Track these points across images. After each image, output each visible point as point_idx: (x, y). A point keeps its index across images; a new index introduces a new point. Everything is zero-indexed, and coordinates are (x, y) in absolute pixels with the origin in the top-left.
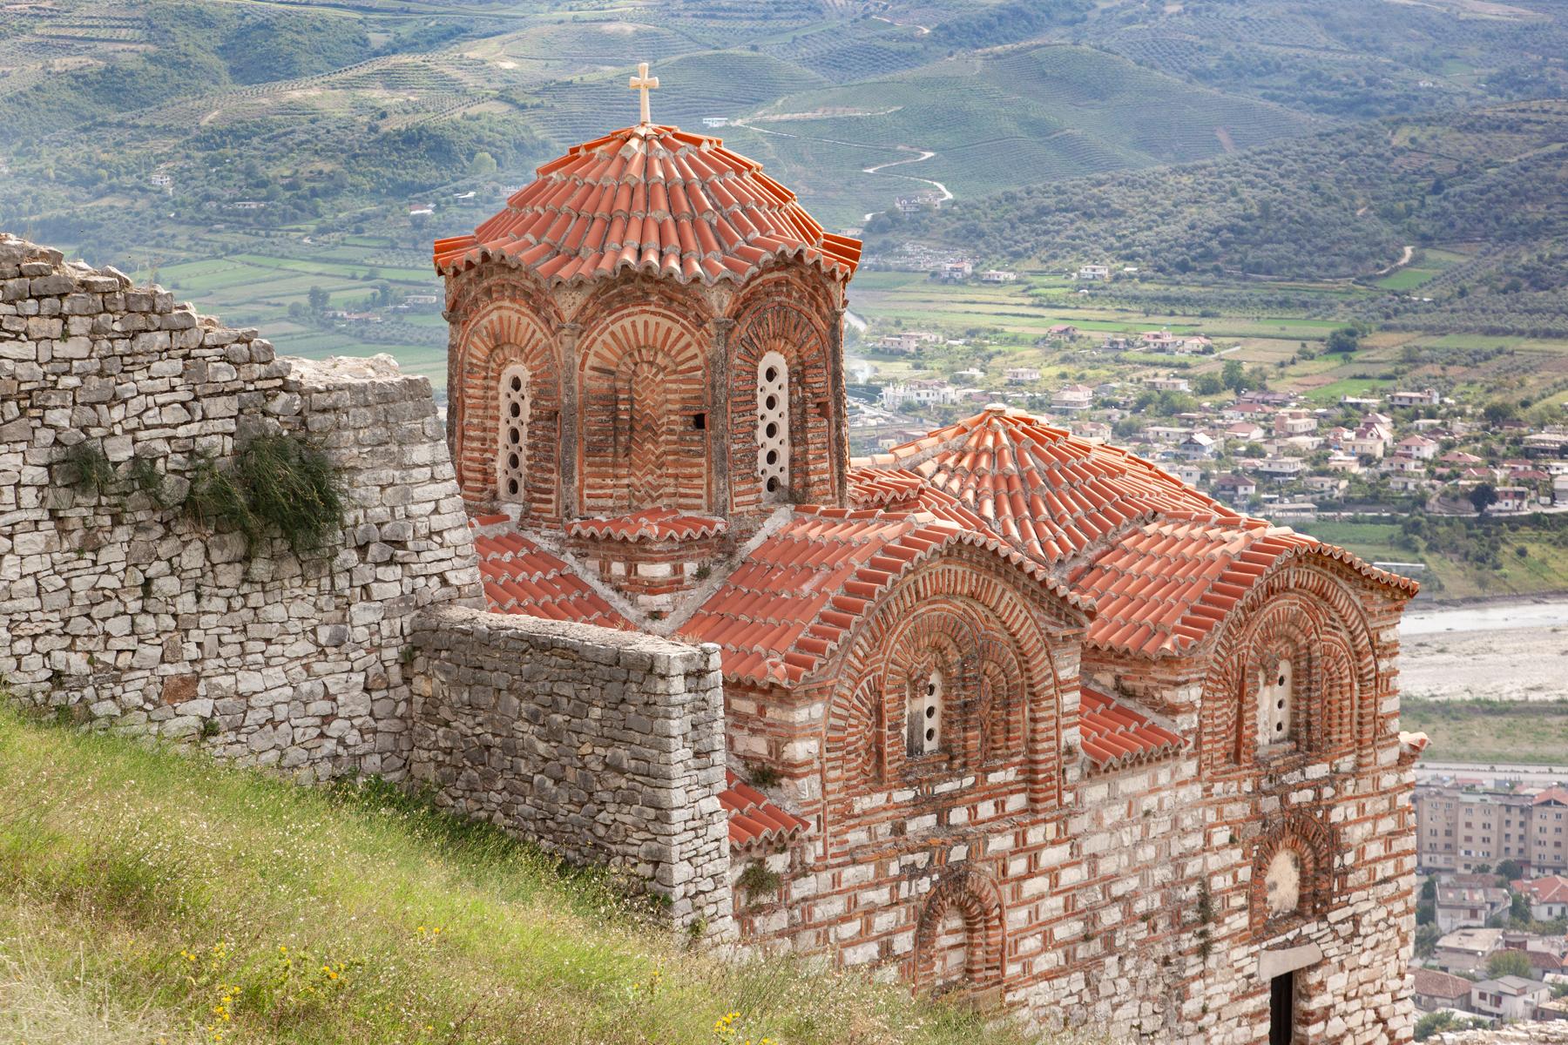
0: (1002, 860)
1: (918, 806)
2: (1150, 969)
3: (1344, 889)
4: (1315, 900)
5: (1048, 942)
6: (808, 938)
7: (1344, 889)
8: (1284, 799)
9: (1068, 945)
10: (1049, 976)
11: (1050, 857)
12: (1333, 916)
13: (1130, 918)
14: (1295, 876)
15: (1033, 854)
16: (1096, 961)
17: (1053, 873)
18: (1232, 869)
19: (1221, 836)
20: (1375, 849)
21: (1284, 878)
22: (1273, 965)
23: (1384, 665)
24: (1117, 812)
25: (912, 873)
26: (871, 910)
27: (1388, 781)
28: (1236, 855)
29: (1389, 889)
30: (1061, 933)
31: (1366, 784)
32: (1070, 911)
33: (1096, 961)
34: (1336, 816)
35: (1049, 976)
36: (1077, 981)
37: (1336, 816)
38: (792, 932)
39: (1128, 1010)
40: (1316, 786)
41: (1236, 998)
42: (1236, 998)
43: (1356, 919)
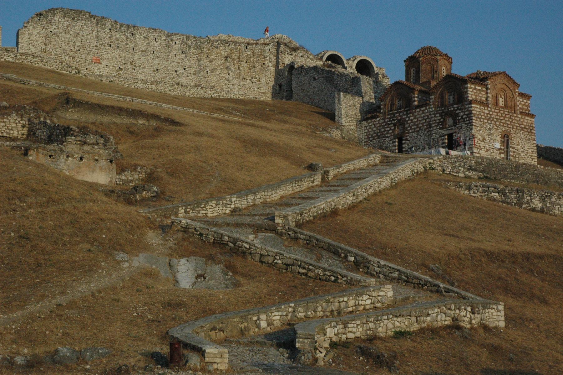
0: (405, 119)
1: (397, 113)
2: (426, 132)
3: (459, 122)
4: (455, 124)
5: (411, 129)
6: (381, 127)
7: (459, 122)
8: (448, 109)
9: (414, 129)
10: (412, 132)
11: (412, 118)
12: (457, 126)
13: (423, 126)
14: (452, 121)
15: (409, 117)
16: (418, 131)
17: (411, 120)
18: (440, 120)
19: (438, 115)
20: (464, 117)
21: (450, 121)
22: (446, 132)
23: (465, 90)
24: (421, 112)
25: (394, 120)
26: (389, 124)
27: (467, 106)
28: (440, 118)
29: (467, 122)
30: (413, 127)
31: (463, 107)
32: (414, 125)
33: (418, 131)
34: (457, 112)
35: (412, 132)
36: (416, 133)
37: (457, 112)
38: (380, 126)
39: (423, 137)
40: (454, 108)
41: (440, 137)
42: (440, 137)
43: (461, 126)
